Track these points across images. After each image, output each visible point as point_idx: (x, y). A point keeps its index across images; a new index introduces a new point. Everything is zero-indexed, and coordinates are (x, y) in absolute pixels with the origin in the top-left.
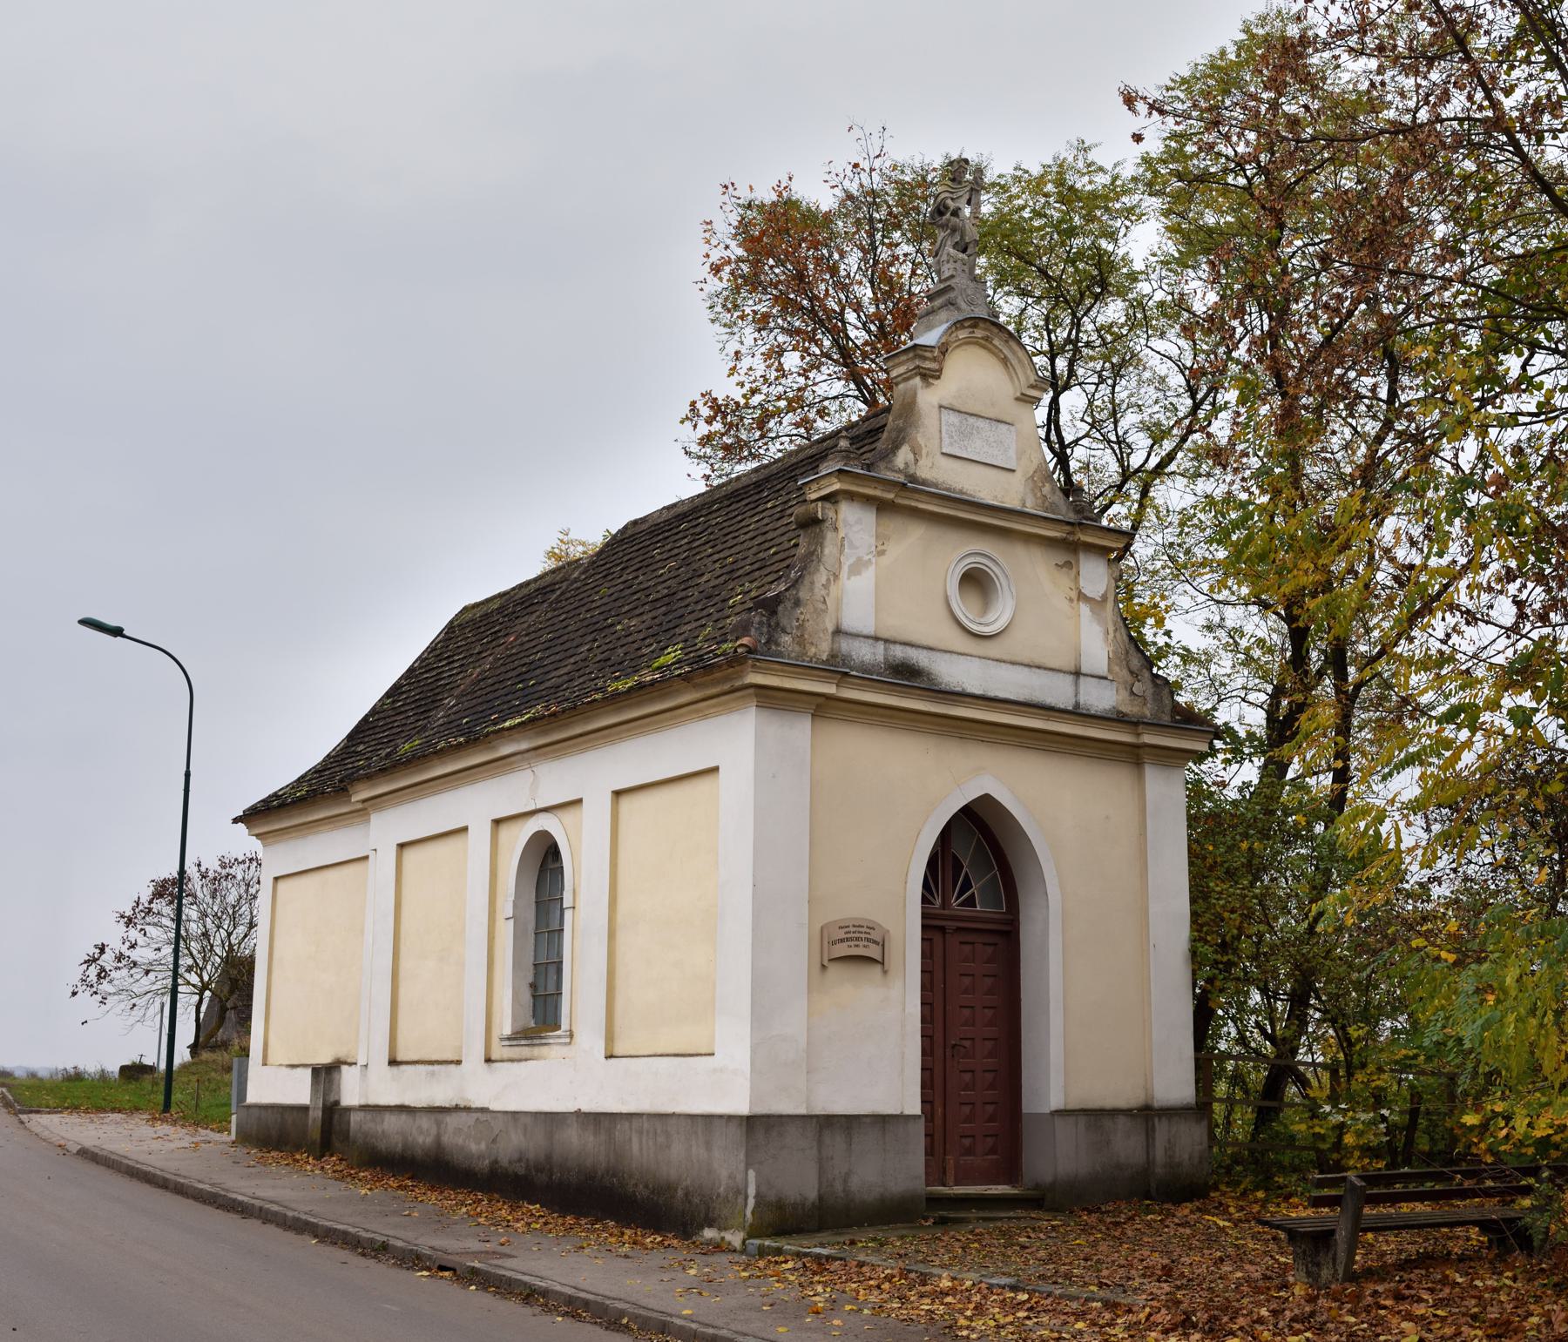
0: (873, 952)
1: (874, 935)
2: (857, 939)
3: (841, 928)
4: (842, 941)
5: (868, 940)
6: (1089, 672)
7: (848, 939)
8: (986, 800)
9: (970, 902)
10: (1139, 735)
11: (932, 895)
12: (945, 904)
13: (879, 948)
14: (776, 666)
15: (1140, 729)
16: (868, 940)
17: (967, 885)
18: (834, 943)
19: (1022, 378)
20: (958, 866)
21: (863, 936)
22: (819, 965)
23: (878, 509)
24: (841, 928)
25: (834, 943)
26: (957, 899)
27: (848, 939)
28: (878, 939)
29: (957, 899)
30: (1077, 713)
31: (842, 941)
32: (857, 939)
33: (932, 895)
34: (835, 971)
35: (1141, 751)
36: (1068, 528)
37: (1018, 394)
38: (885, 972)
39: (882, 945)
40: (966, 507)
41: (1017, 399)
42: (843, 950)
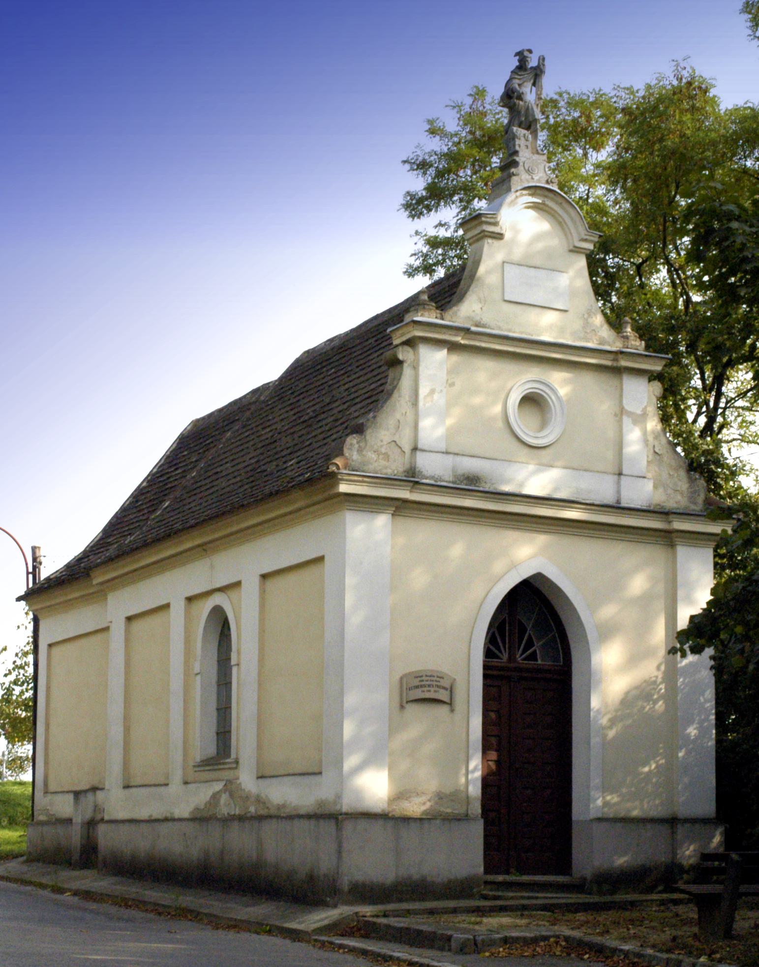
0: (443, 695)
1: (443, 683)
2: (429, 686)
3: (417, 677)
4: (417, 687)
5: (438, 686)
6: (629, 473)
7: (422, 686)
8: (539, 576)
9: (533, 657)
10: (670, 522)
11: (501, 652)
12: (511, 658)
13: (448, 692)
14: (356, 478)
15: (671, 517)
16: (438, 686)
17: (530, 644)
18: (410, 689)
19: (575, 235)
20: (523, 630)
21: (434, 683)
22: (398, 705)
23: (449, 350)
24: (417, 677)
25: (410, 689)
26: (521, 655)
27: (422, 686)
28: (448, 686)
29: (521, 655)
30: (617, 508)
31: (417, 687)
32: (429, 686)
33: (501, 652)
34: (412, 709)
35: (674, 535)
36: (612, 356)
37: (571, 247)
38: (452, 711)
39: (451, 690)
40: (523, 344)
41: (571, 251)
42: (418, 693)
